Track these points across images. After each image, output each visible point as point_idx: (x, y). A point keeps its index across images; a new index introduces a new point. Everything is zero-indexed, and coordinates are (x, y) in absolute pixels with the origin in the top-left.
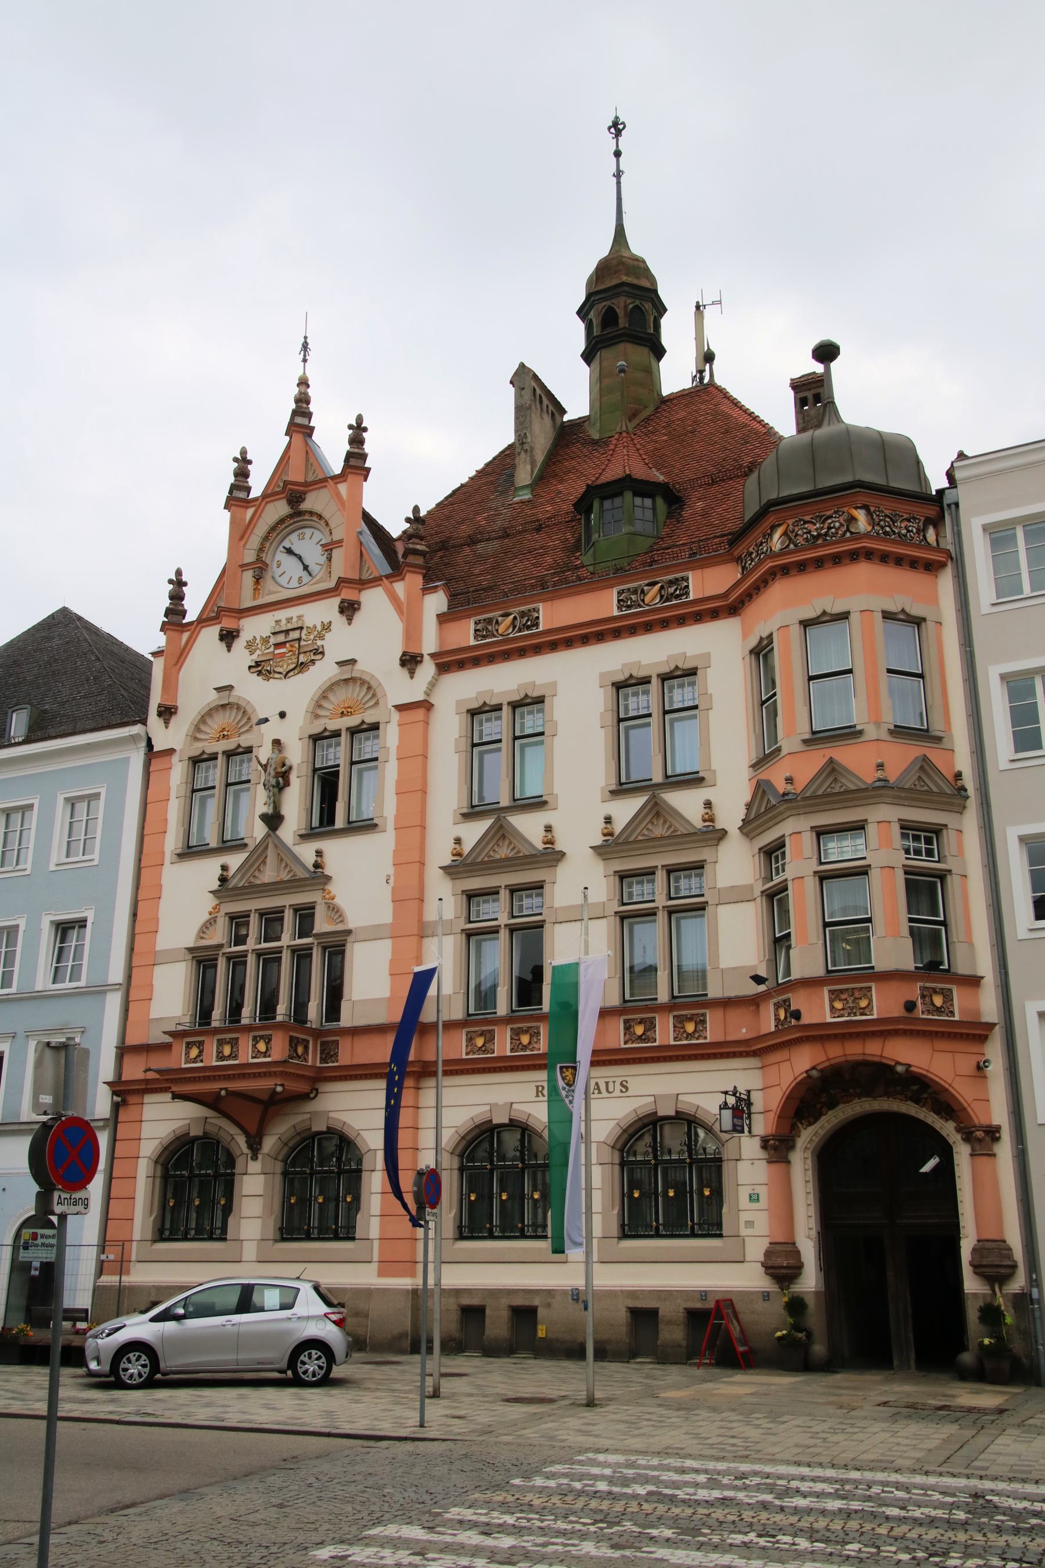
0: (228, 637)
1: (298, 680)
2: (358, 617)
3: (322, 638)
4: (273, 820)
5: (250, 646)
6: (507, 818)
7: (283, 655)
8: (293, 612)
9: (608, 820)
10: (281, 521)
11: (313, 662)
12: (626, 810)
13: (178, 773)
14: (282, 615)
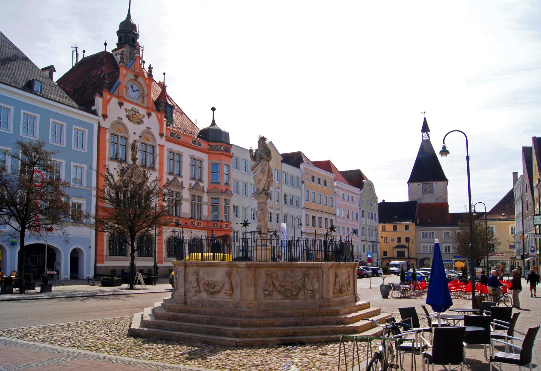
0: (121, 104)
1: (136, 126)
2: (151, 117)
3: (143, 118)
4: (134, 159)
5: (126, 109)
6: (178, 178)
7: (135, 118)
8: (137, 108)
9: (191, 184)
10: (132, 79)
11: (141, 123)
12: (193, 183)
13: (108, 136)
14: (135, 107)
